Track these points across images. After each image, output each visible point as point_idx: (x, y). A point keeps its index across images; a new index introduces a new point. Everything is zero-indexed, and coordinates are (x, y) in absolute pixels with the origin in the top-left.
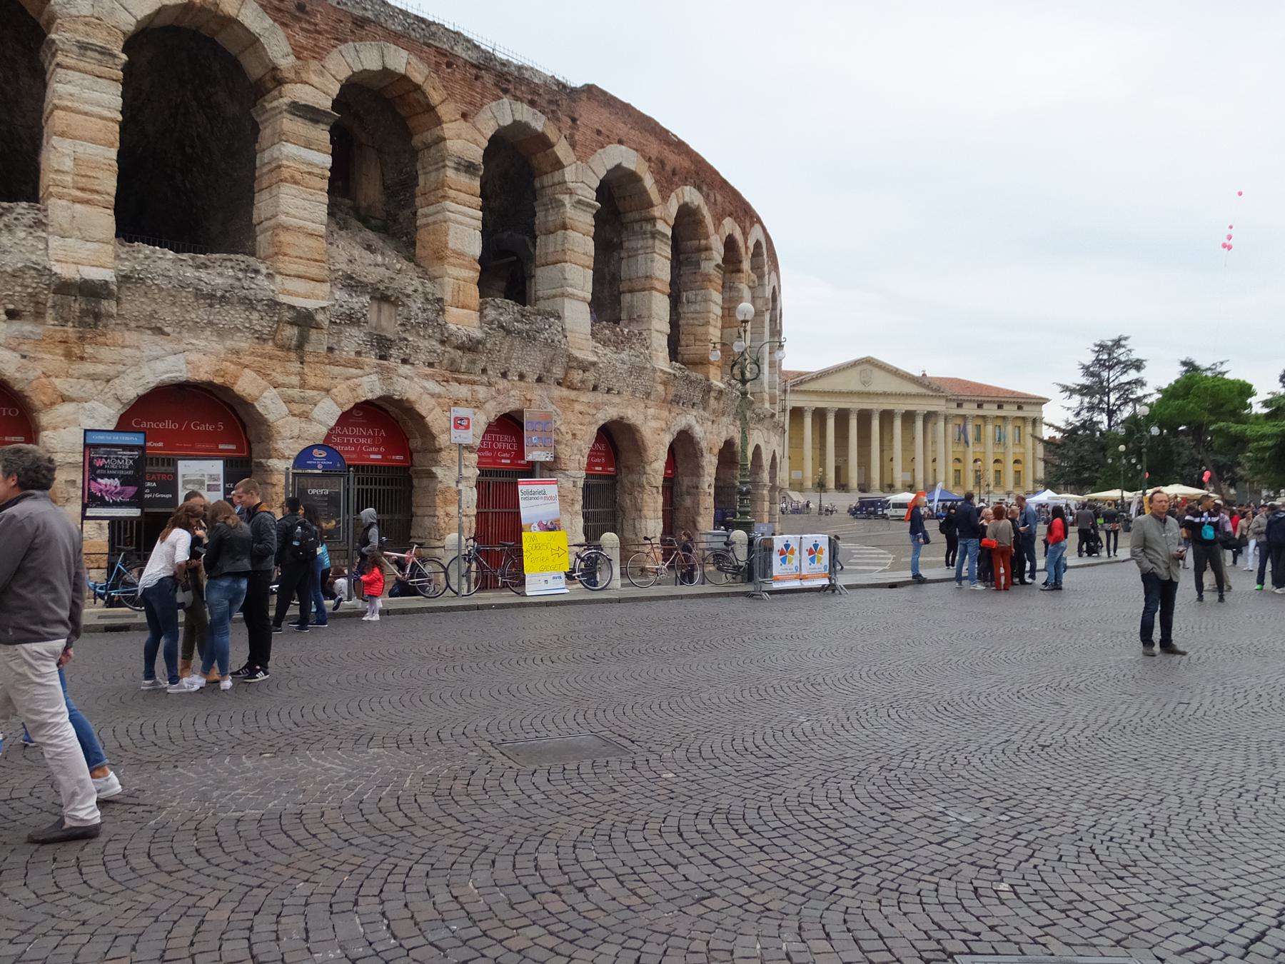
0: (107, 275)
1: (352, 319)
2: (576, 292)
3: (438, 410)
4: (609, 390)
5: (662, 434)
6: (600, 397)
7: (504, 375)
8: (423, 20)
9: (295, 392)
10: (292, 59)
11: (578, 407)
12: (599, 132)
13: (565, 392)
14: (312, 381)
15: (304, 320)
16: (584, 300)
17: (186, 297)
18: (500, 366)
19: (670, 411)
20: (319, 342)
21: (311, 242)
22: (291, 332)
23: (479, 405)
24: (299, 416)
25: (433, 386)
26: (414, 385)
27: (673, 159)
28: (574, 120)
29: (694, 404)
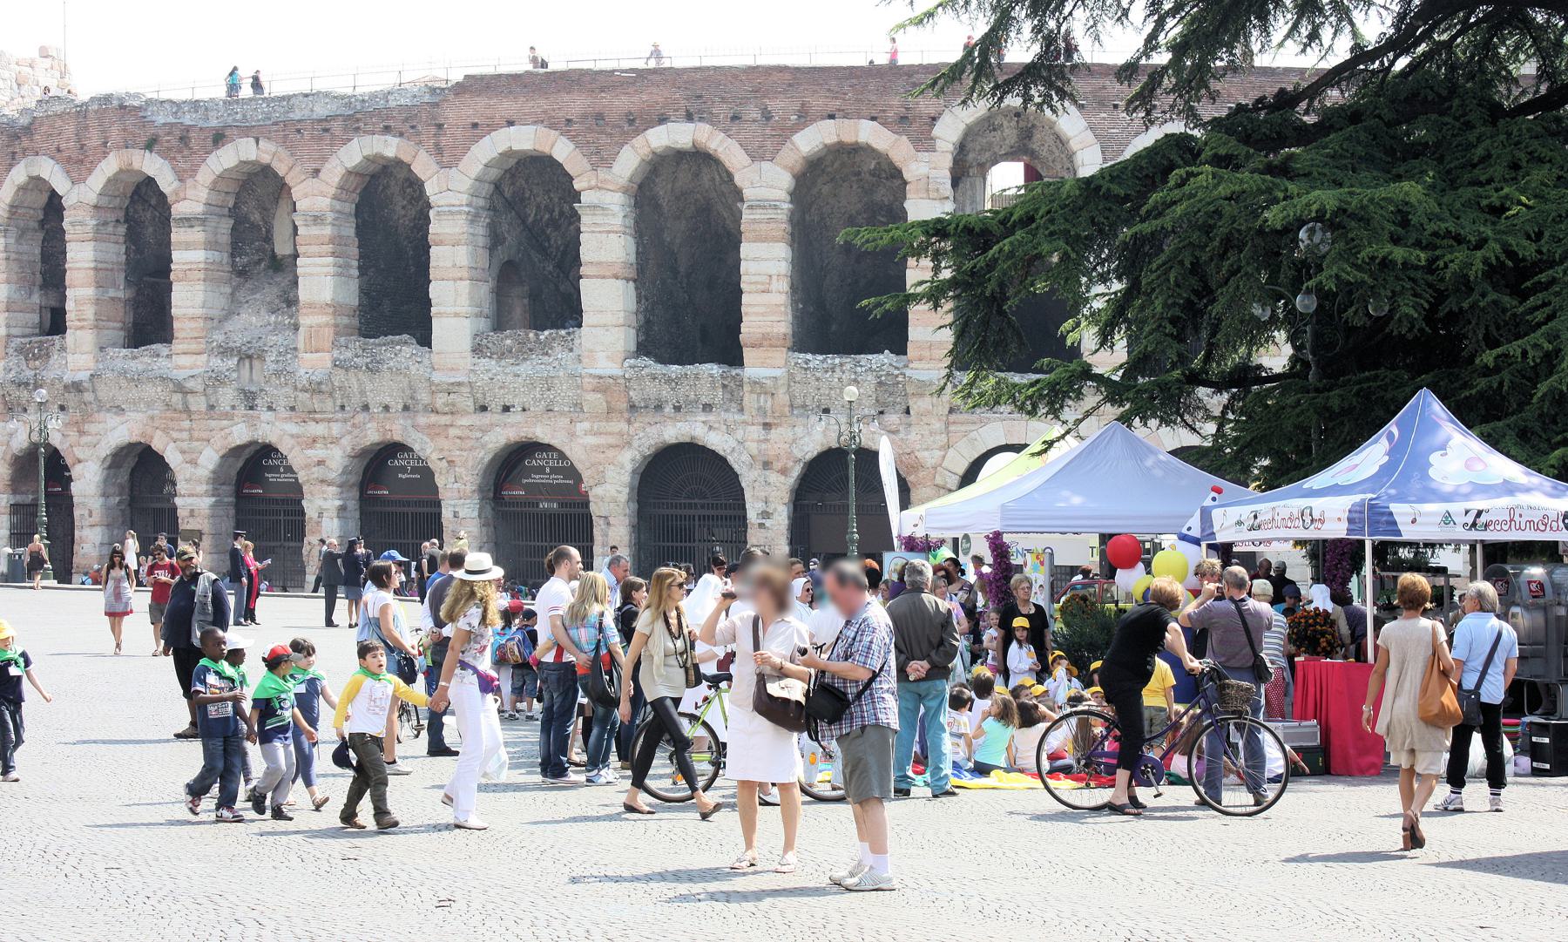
0: (83, 376)
1: (217, 380)
2: (442, 309)
3: (297, 448)
4: (506, 409)
5: (611, 453)
6: (486, 418)
7: (366, 408)
8: (283, 98)
9: (185, 445)
10: (176, 184)
11: (452, 432)
12: (475, 125)
13: (434, 418)
14: (196, 434)
15: (180, 388)
16: (456, 315)
17: (124, 383)
18: (356, 401)
19: (629, 422)
20: (198, 403)
21: (193, 325)
22: (177, 398)
23: (335, 441)
24: (190, 462)
25: (292, 428)
26: (274, 429)
27: (620, 103)
28: (440, 126)
29: (707, 408)
